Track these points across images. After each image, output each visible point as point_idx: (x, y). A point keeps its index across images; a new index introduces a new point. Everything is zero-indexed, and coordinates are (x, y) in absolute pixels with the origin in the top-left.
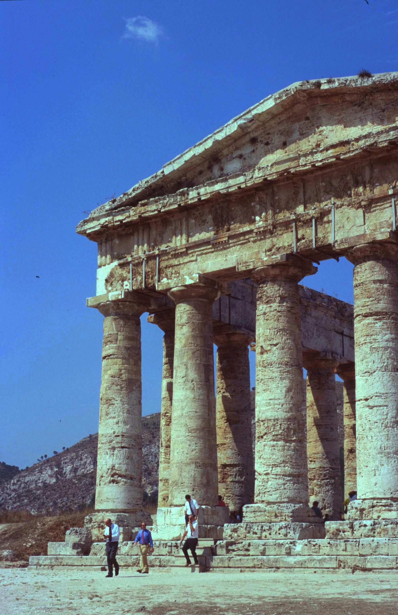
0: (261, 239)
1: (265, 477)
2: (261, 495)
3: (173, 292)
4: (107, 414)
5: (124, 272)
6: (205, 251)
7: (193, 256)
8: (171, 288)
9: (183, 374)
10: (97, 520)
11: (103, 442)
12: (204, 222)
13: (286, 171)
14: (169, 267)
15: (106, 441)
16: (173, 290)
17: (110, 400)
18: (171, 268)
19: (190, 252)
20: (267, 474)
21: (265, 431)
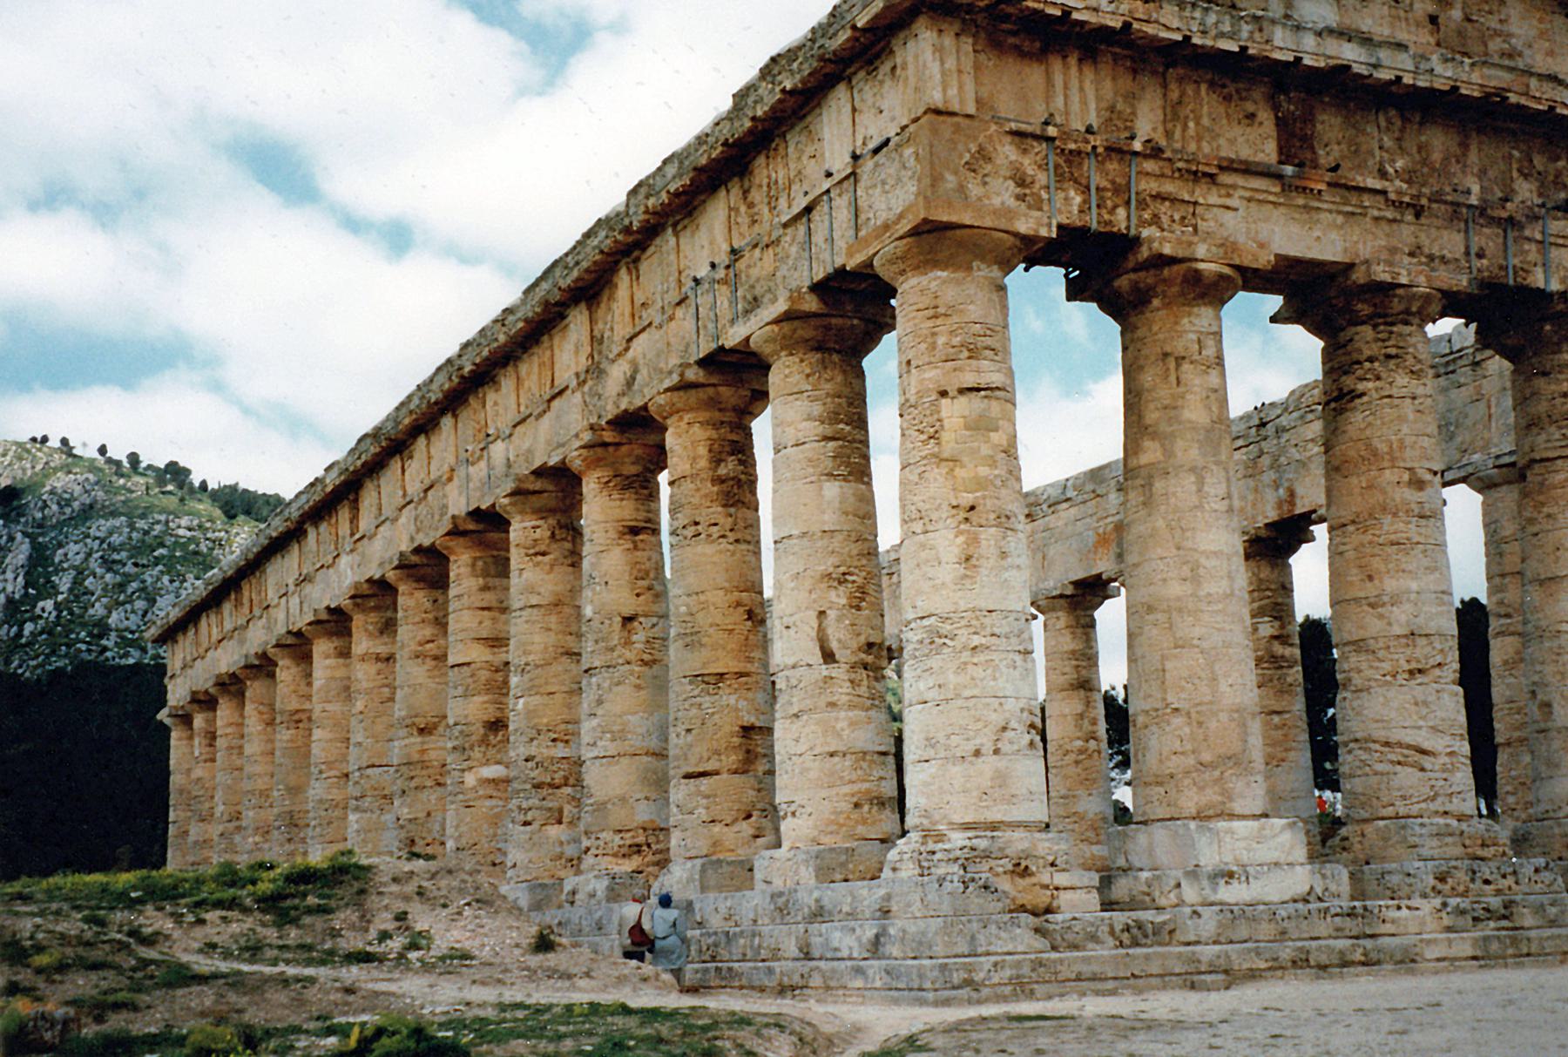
0: (1394, 221)
1: (1447, 760)
2: (1440, 800)
3: (1197, 271)
4: (1004, 555)
5: (1026, 161)
6: (1261, 197)
7: (1229, 195)
8: (1196, 260)
9: (1221, 490)
10: (1008, 852)
11: (997, 631)
12: (1251, 116)
13: (1501, 93)
14: (1164, 199)
15: (1007, 629)
16: (1201, 266)
17: (1008, 517)
18: (1167, 203)
19: (1226, 178)
20: (1451, 754)
21: (1439, 659)
